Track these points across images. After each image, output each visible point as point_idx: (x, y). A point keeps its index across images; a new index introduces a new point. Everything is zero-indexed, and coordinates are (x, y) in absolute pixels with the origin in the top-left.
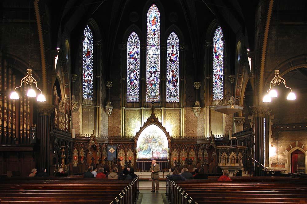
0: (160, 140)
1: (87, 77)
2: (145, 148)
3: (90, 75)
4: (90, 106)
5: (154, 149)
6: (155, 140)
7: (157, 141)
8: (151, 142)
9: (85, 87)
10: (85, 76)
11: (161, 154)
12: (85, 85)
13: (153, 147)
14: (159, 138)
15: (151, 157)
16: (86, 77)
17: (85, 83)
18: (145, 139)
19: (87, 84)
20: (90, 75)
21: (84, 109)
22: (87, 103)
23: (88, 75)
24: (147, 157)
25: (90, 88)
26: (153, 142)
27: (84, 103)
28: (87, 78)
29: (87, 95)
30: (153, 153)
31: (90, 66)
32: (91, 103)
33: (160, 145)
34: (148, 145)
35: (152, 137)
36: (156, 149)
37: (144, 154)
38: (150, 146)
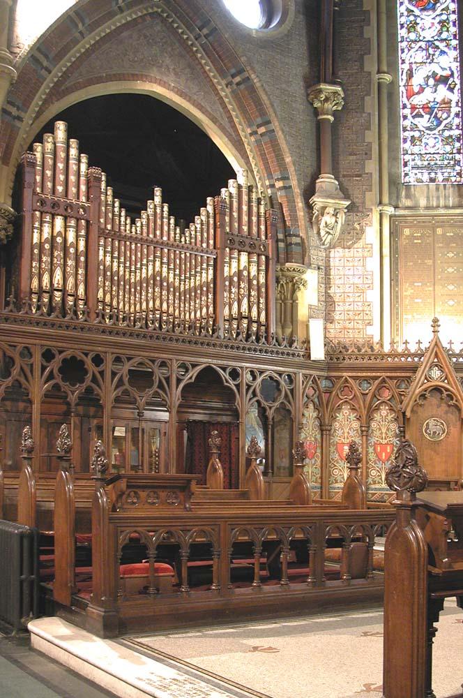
1: (428, 91)
3: (444, 80)
4: (442, 211)
9: (417, 134)
10: (416, 89)
12: (414, 127)
16: (422, 90)
17: (413, 117)
19: (423, 122)
20: (444, 80)
21: (407, 232)
22: (423, 202)
23: (431, 82)
25: (447, 133)
27: (408, 203)
28: (426, 97)
29: (429, 168)
31: (442, 40)
32: (446, 197)
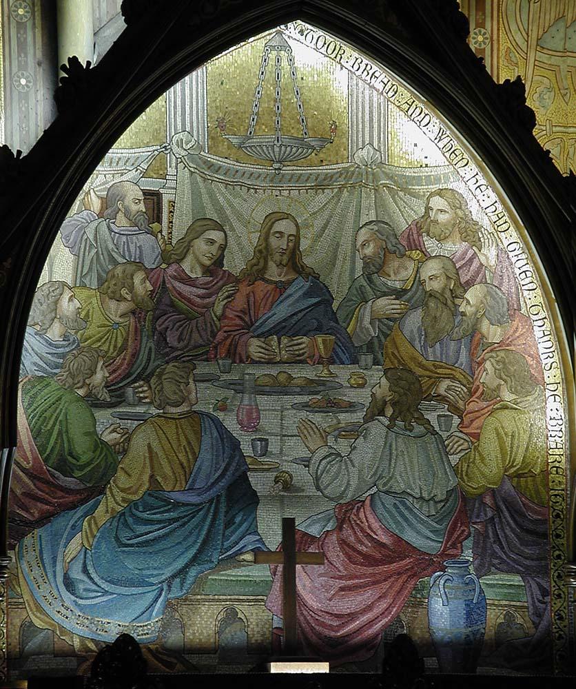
0: (414, 321)
2: (144, 445)
5: (302, 476)
6: (320, 314)
7: (364, 324)
8: (255, 347)
11: (428, 564)
13: (283, 435)
14: (400, 274)
15: (260, 618)
18: (142, 286)
24: (174, 638)
26: (281, 347)
30: (294, 549)
33: (408, 400)
34: (204, 397)
35: (264, 252)
36: (347, 481)
37: (132, 565)
38: (230, 423)
